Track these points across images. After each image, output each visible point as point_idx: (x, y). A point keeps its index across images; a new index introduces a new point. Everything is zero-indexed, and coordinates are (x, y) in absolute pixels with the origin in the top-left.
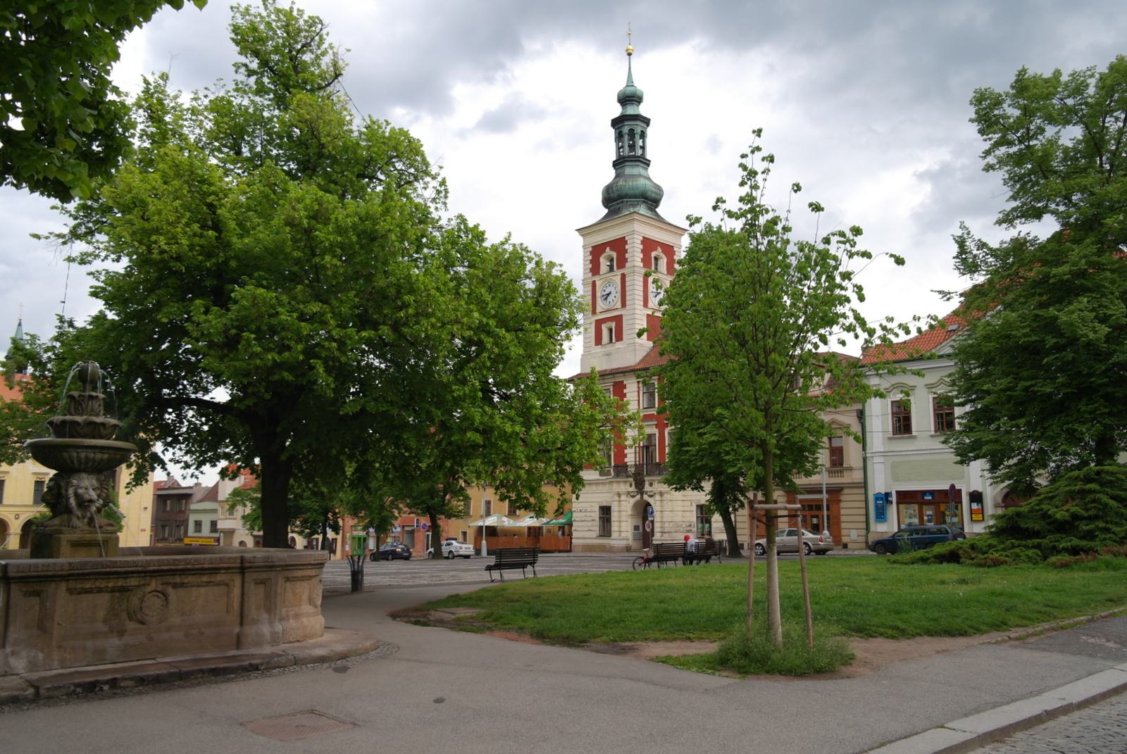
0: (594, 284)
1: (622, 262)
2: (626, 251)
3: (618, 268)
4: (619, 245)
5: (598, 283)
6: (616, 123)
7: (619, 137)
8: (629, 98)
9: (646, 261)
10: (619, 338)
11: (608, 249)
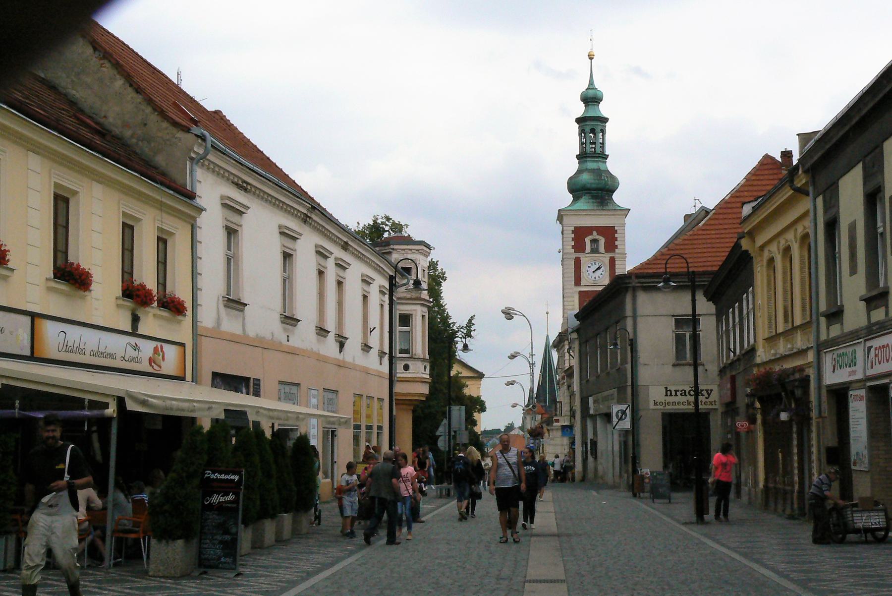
0: (578, 262)
2: (616, 239)
5: (583, 260)
6: (578, 121)
7: (582, 131)
8: (591, 99)
11: (595, 233)
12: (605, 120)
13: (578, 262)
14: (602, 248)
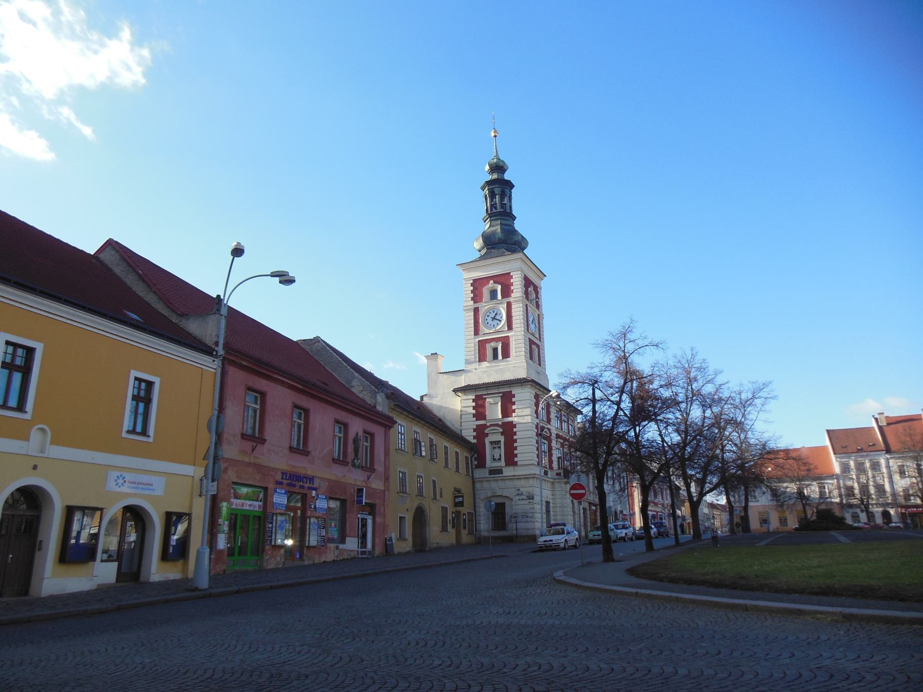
1: (507, 292)
3: (504, 296)
4: (504, 280)
8: (498, 168)
9: (526, 293)
10: (506, 355)
11: (491, 282)
12: (509, 185)
13: (476, 311)
14: (499, 297)
